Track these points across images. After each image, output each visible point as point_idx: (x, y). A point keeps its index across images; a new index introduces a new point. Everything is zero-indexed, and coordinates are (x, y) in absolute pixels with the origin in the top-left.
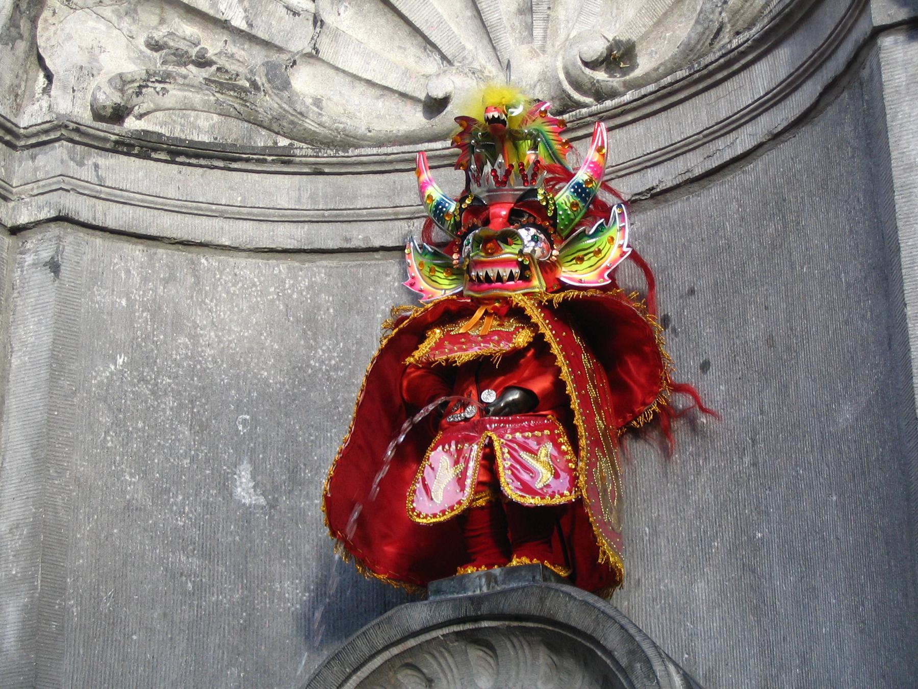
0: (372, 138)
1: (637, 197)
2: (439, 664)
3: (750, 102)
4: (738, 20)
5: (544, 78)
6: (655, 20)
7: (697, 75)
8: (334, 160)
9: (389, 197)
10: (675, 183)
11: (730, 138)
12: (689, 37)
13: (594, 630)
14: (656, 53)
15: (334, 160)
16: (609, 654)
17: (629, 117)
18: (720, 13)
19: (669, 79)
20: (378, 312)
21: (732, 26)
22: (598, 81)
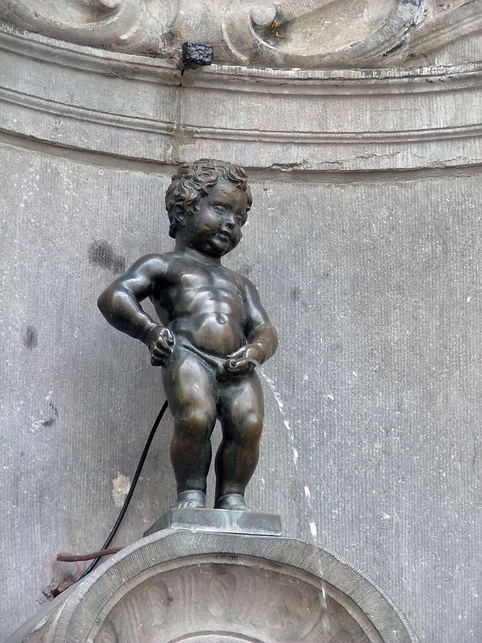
0: (35, 22)
1: (278, 167)
2: (184, 588)
3: (426, 127)
4: (418, 44)
5: (205, 21)
6: (321, 5)
7: (373, 82)
8: (10, 37)
9: (45, 88)
10: (322, 168)
11: (389, 150)
12: (367, 41)
13: (353, 592)
14: (311, 35)
15: (10, 37)
16: (365, 616)
17: (286, 92)
18: (406, 33)
19: (340, 73)
20: (21, 201)
21: (410, 48)
22: (262, 46)
